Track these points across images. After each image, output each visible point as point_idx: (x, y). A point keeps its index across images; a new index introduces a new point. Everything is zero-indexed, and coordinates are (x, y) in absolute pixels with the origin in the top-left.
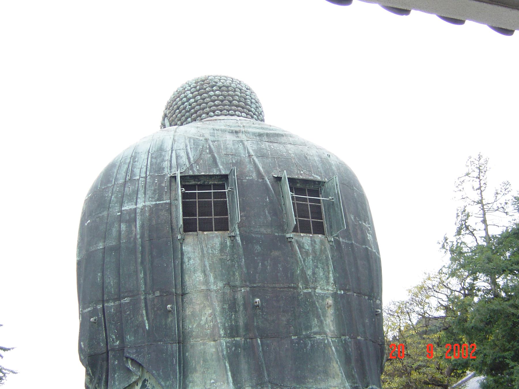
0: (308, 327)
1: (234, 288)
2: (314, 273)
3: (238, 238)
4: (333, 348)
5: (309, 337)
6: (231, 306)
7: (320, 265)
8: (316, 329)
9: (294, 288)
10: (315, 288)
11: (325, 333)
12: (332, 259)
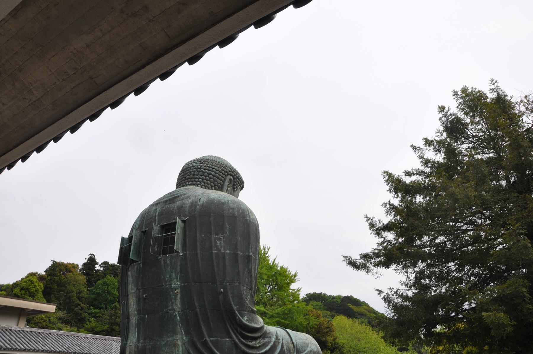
0: (167, 307)
1: (139, 290)
2: (170, 276)
3: (141, 265)
4: (178, 318)
5: (167, 312)
6: (139, 300)
7: (173, 271)
8: (170, 308)
9: (161, 286)
10: (171, 284)
11: (174, 310)
12: (180, 266)
